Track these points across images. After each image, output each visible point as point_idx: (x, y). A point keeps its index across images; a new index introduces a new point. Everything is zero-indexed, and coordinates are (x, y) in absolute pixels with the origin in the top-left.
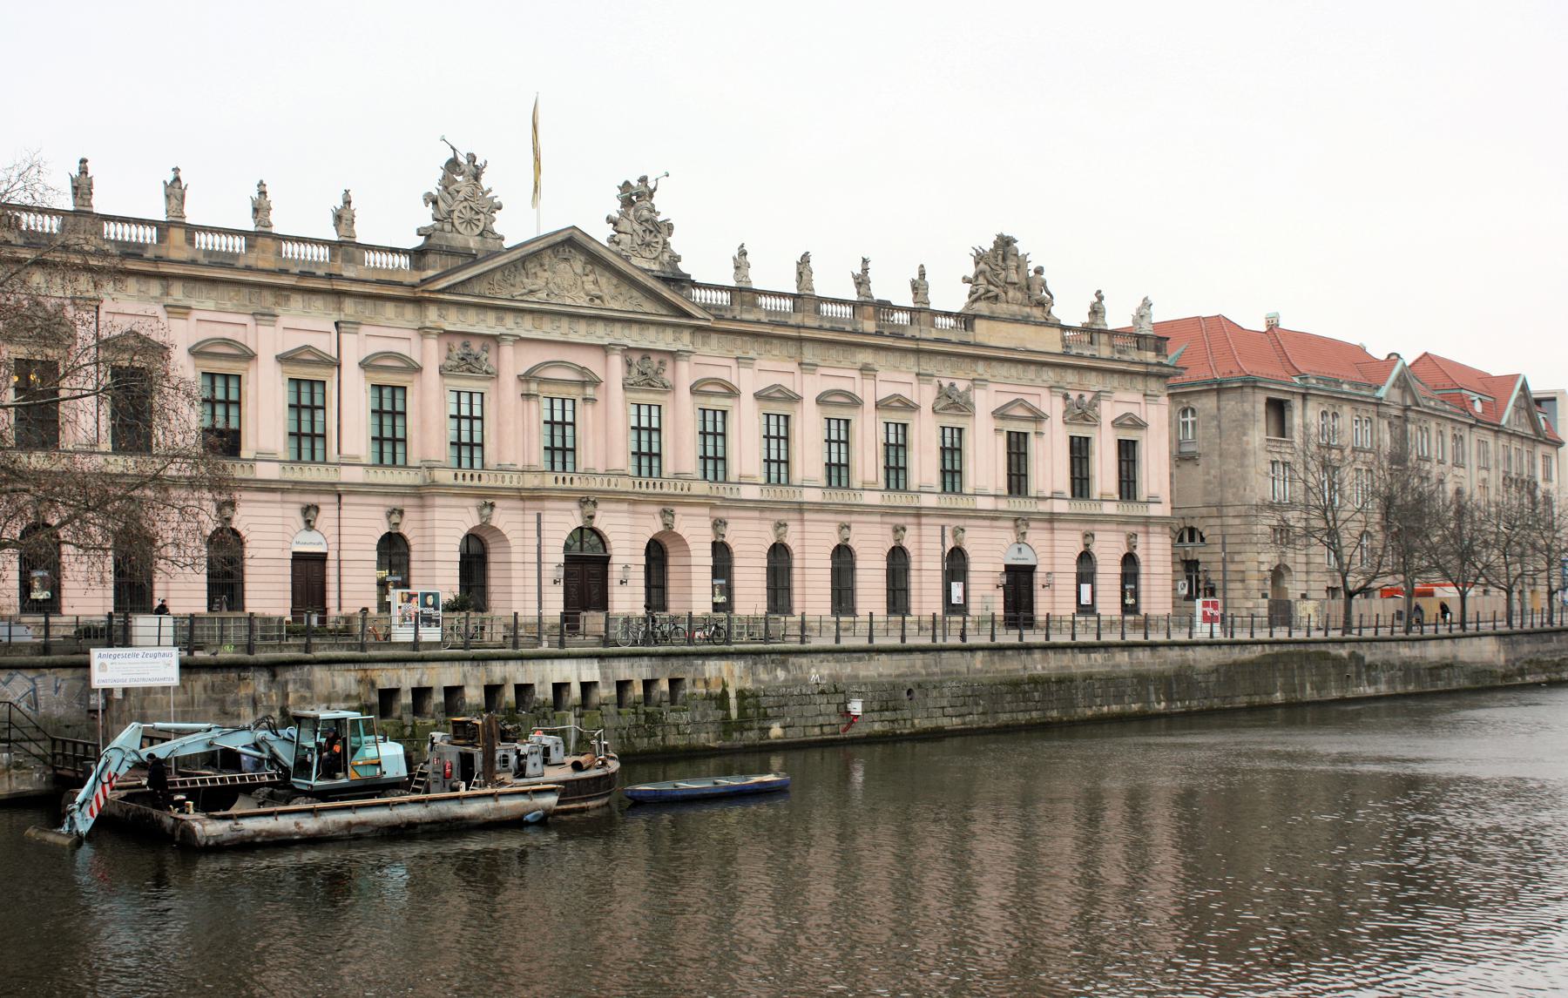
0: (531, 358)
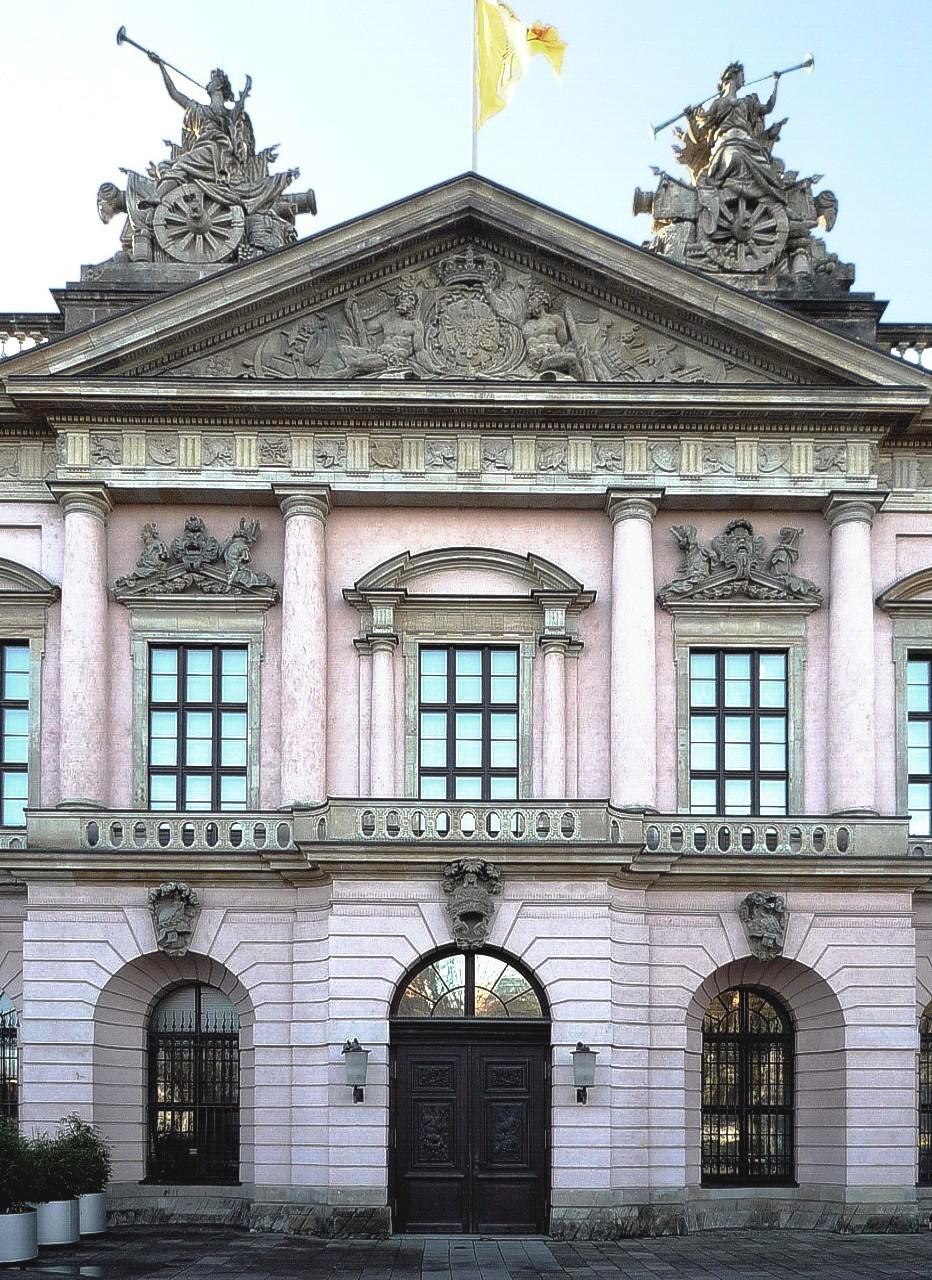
0: (369, 547)
